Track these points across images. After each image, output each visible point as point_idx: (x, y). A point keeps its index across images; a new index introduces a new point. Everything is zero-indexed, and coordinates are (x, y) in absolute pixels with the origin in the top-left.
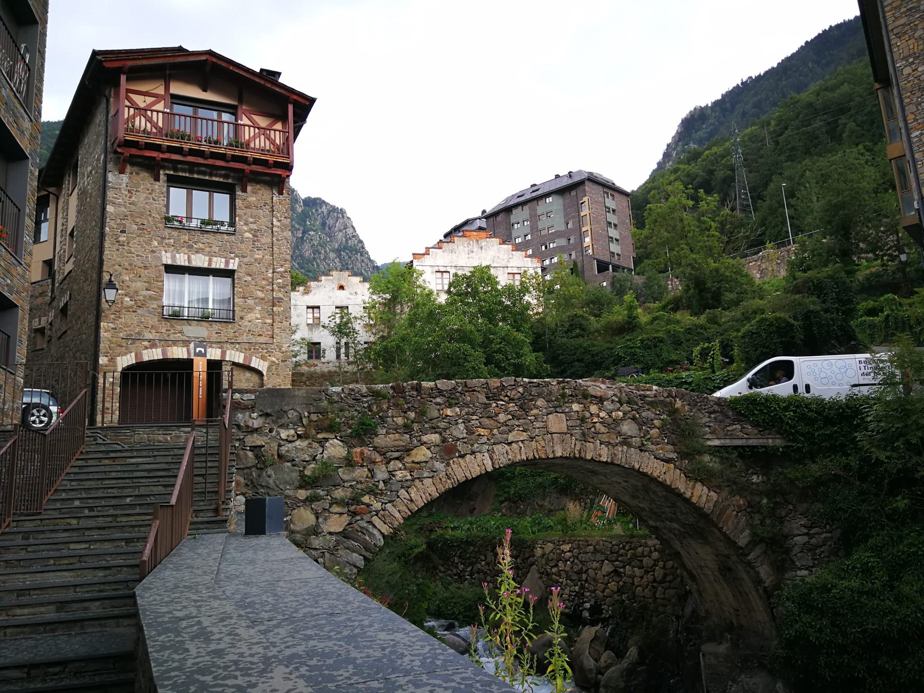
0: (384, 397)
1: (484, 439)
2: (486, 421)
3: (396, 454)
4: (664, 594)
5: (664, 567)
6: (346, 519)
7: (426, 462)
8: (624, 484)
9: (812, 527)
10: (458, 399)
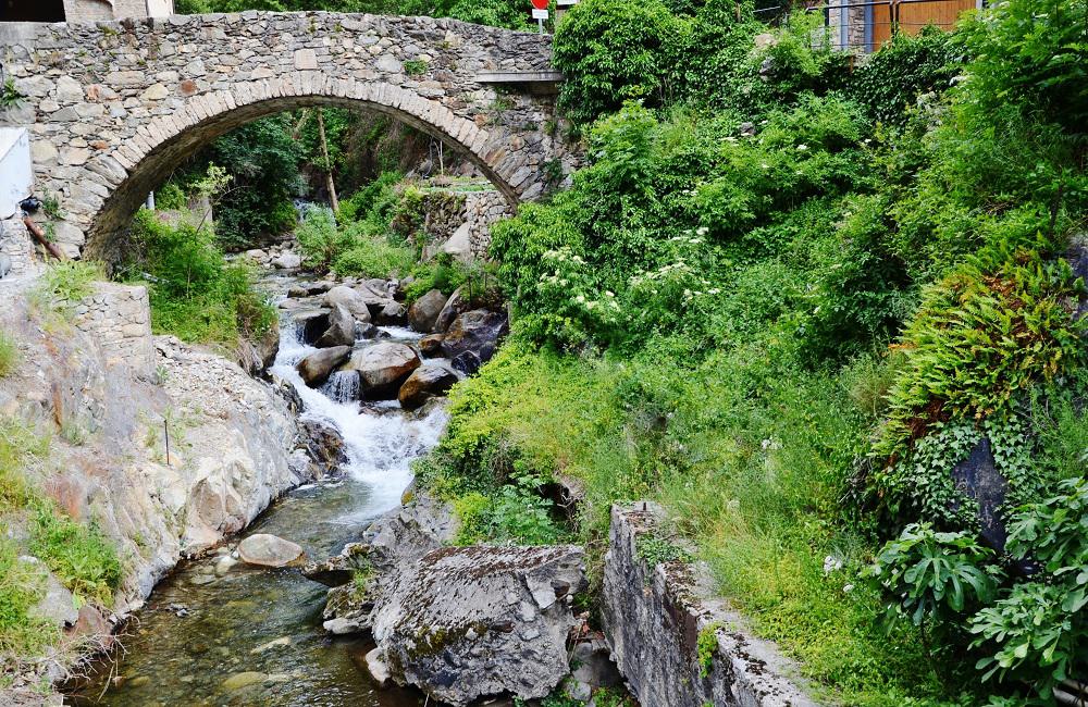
2: (225, 58)
6: (87, 153)
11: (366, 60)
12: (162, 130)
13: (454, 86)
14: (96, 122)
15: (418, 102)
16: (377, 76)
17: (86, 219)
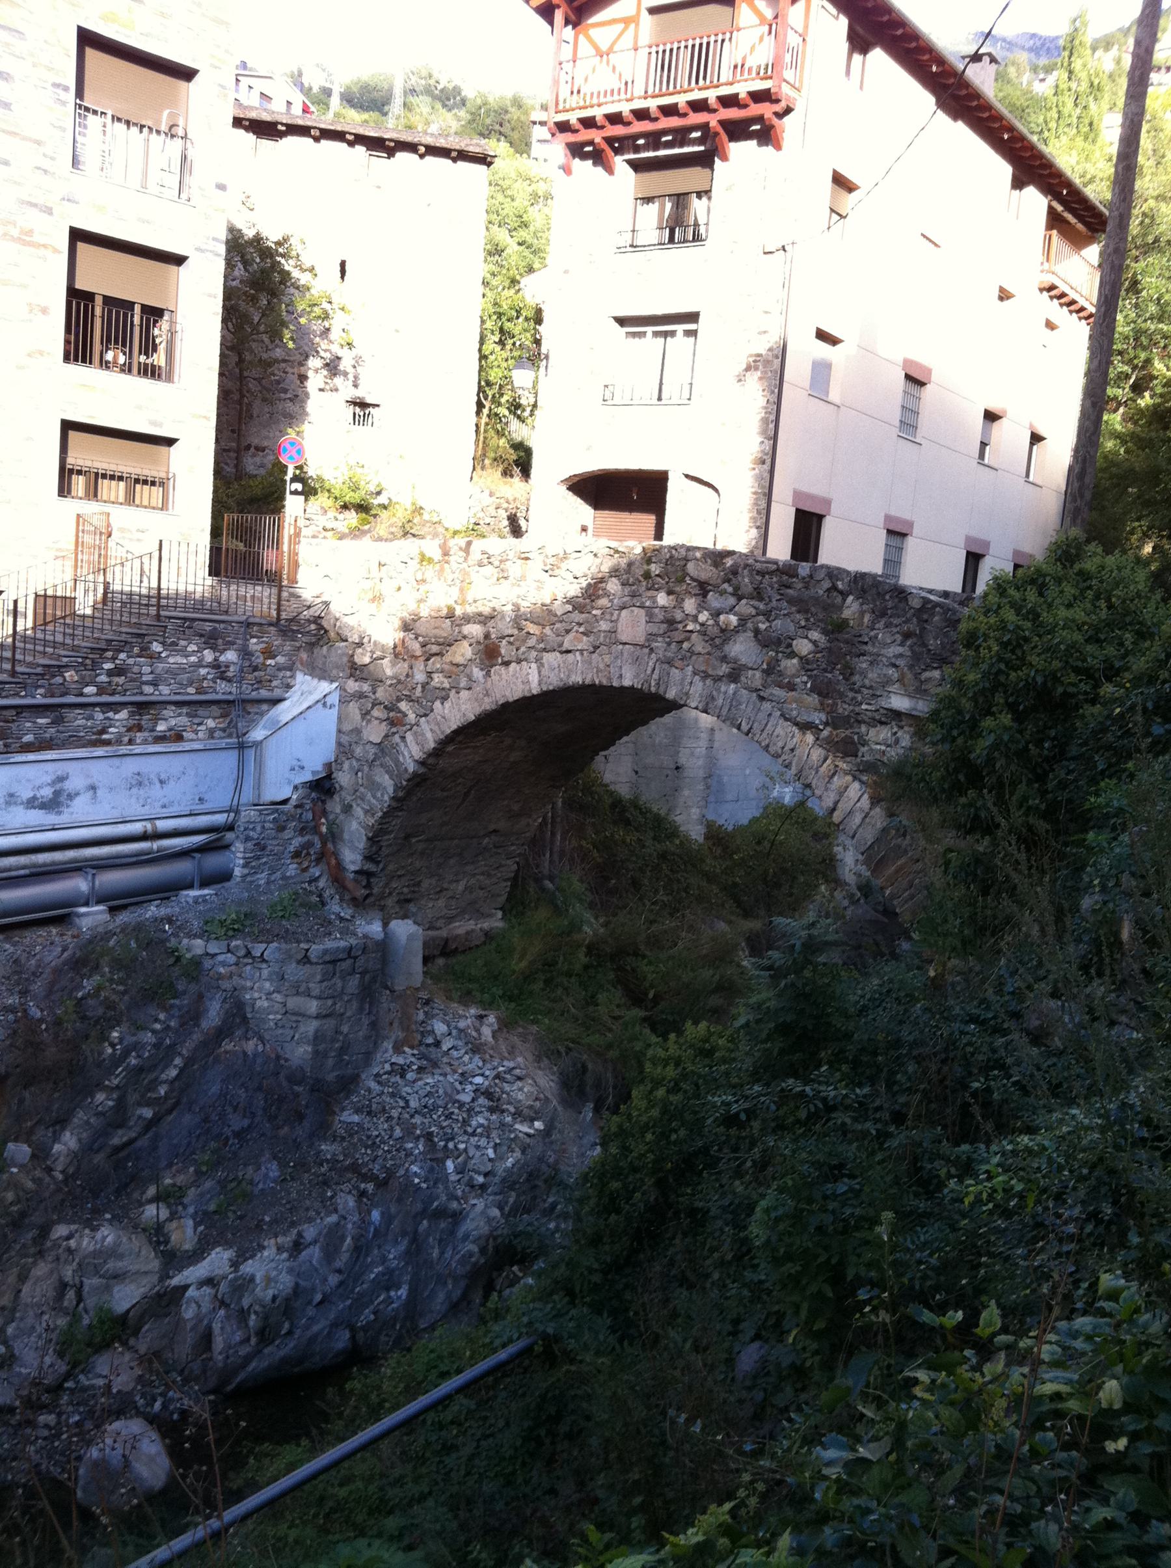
1: (532, 642)
6: (384, 727)
13: (844, 709)
16: (724, 669)
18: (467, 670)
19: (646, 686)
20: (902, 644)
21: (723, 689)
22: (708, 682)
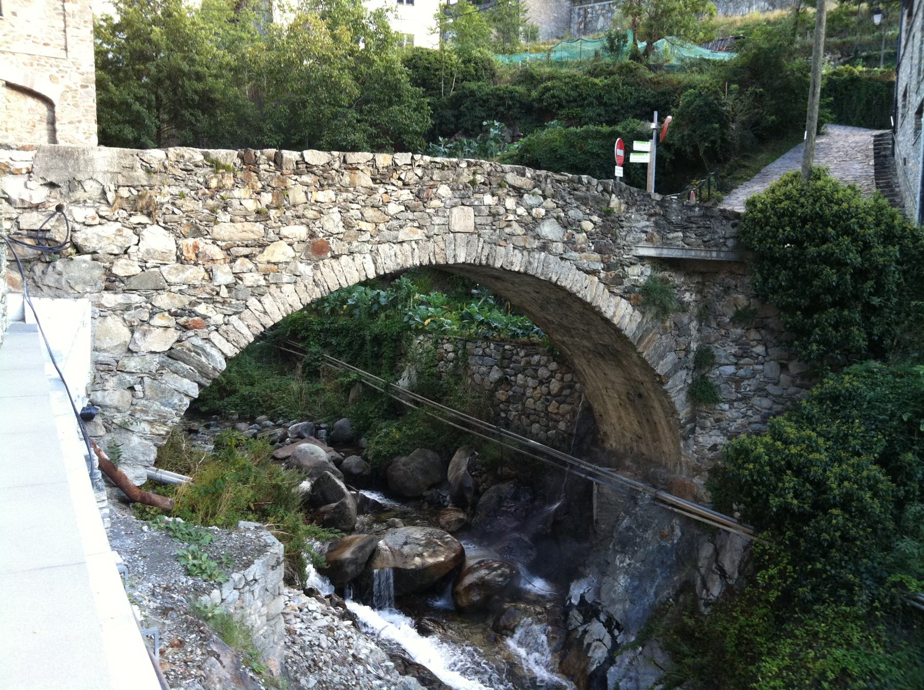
0: (227, 168)
1: (366, 237)
2: (369, 213)
3: (246, 251)
4: (558, 408)
5: (562, 380)
6: (173, 335)
7: (287, 263)
8: (535, 294)
9: (742, 357)
10: (333, 179)
11: (527, 225)
12: (281, 304)
13: (613, 259)
14: (192, 292)
15: (577, 277)
16: (536, 244)
17: (163, 430)
18: (291, 267)
19: (477, 262)
20: (648, 220)
21: (537, 256)
22: (525, 253)
